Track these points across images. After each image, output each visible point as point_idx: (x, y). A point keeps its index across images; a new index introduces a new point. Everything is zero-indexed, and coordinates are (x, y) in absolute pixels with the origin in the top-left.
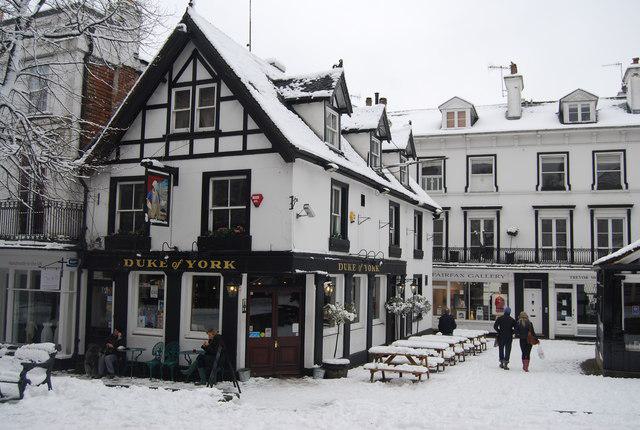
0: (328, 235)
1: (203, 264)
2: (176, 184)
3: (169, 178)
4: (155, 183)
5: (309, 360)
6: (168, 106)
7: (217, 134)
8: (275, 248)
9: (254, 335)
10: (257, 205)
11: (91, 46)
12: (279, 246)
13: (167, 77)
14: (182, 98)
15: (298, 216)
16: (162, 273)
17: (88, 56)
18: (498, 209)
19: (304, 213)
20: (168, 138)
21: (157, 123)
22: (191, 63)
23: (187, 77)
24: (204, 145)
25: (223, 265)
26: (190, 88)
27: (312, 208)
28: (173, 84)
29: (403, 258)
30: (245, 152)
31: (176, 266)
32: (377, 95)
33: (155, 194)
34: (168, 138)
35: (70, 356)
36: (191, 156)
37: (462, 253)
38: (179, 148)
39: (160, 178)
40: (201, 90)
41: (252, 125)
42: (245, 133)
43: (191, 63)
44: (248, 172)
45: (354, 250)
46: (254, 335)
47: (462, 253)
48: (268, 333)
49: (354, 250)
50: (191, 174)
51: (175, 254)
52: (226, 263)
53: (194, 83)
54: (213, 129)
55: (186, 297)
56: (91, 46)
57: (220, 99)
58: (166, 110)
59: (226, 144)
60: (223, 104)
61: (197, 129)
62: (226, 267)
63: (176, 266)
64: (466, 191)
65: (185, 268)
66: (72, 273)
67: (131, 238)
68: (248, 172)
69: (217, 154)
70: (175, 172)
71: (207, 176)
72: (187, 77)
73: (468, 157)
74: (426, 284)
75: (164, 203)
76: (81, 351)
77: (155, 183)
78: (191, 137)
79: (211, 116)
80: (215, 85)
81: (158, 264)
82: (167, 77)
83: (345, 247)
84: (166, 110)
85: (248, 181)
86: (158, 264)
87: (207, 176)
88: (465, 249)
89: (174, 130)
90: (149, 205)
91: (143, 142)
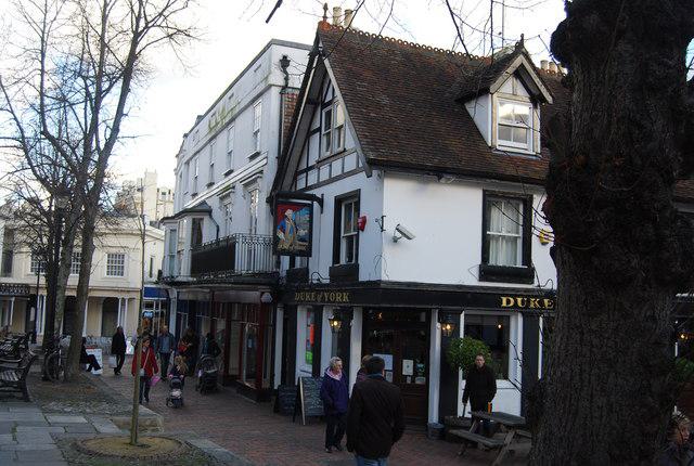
0: (479, 261)
3: (311, 206)
4: (289, 213)
5: (434, 416)
6: (319, 129)
11: (286, 79)
12: (373, 278)
15: (395, 240)
19: (398, 235)
20: (320, 162)
21: (314, 153)
27: (408, 227)
28: (325, 105)
33: (289, 225)
34: (320, 162)
36: (332, 180)
38: (324, 174)
51: (320, 288)
56: (286, 79)
69: (344, 175)
70: (321, 202)
72: (329, 98)
77: (289, 213)
85: (358, 204)
90: (281, 235)
91: (309, 169)
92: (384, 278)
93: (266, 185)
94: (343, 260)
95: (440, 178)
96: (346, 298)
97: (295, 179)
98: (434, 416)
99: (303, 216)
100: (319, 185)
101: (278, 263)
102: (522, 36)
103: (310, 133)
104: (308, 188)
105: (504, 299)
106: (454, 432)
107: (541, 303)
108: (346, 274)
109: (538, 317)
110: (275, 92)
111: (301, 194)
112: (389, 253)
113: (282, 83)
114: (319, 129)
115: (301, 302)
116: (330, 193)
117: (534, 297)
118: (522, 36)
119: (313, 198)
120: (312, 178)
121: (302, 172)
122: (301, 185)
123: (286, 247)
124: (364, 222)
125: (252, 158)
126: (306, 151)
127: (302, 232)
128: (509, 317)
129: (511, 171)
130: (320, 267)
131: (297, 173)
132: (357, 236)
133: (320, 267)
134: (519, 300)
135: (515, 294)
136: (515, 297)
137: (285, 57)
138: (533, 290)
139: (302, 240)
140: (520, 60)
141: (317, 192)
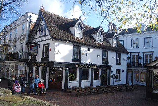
2: (40, 47)
3: (37, 46)
4: (33, 47)
5: (63, 88)
7: (45, 36)
18: (153, 52)
20: (39, 37)
21: (38, 34)
23: (42, 24)
24: (44, 38)
25: (45, 65)
28: (41, 26)
29: (109, 65)
30: (49, 39)
33: (33, 49)
34: (39, 37)
37: (143, 64)
38: (40, 39)
44: (49, 44)
46: (51, 81)
47: (143, 64)
50: (42, 44)
53: (43, 25)
55: (40, 72)
59: (47, 38)
64: (144, 47)
66: (26, 67)
67: (34, 59)
68: (49, 44)
69: (45, 40)
70: (39, 45)
71: (44, 45)
72: (42, 24)
73: (144, 38)
77: (33, 47)
78: (42, 37)
85: (49, 46)
87: (44, 45)
88: (144, 63)
90: (31, 52)
91: (36, 38)
92: (55, 61)
93: (25, 41)
94: (44, 56)
95: (66, 42)
96: (45, 65)
97: (33, 40)
98: (63, 88)
99: (36, 48)
100: (39, 42)
101: (28, 57)
102: (80, 16)
103: (37, 31)
104: (36, 42)
105: (76, 65)
106: (69, 91)
107: (82, 66)
108: (46, 59)
109: (82, 69)
111: (34, 43)
114: (39, 31)
116: (42, 44)
117: (81, 65)
118: (80, 16)
119: (38, 44)
120: (37, 40)
121: (35, 39)
122: (34, 41)
123: (32, 54)
125: (22, 35)
127: (36, 51)
129: (78, 41)
130: (39, 58)
131: (33, 39)
132: (48, 53)
133: (39, 58)
134: (79, 65)
135: (78, 64)
136: (78, 65)
137: (31, 15)
138: (81, 64)
140: (80, 21)
141: (39, 43)
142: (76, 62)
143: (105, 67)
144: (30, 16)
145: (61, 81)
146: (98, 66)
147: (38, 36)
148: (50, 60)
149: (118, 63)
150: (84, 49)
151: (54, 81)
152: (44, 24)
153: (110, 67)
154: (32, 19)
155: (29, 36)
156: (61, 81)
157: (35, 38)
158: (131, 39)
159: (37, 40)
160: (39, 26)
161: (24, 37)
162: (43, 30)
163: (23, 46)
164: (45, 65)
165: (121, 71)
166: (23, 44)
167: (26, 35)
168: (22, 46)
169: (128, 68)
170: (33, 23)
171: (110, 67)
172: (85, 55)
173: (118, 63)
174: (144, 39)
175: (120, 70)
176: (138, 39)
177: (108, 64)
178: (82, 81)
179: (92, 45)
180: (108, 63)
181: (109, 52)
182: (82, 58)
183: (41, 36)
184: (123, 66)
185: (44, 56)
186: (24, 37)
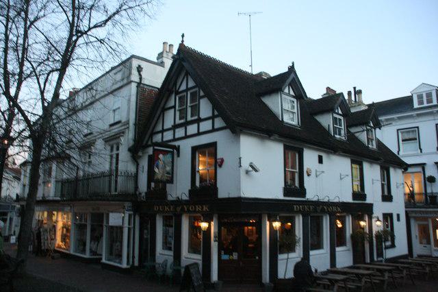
0: (283, 185)
1: (192, 208)
2: (178, 156)
3: (173, 153)
4: (161, 156)
6: (174, 107)
7: (199, 121)
8: (231, 196)
9: (225, 257)
10: (220, 166)
11: (141, 79)
12: (233, 195)
13: (174, 89)
14: (182, 101)
16: (171, 214)
17: (139, 84)
19: (250, 169)
20: (175, 127)
21: (170, 119)
22: (186, 78)
23: (183, 87)
24: (192, 129)
25: (202, 208)
26: (185, 94)
29: (368, 201)
30: (214, 130)
31: (179, 209)
32: (355, 88)
33: (160, 163)
34: (175, 127)
35: (129, 267)
36: (186, 137)
38: (180, 133)
39: (165, 153)
40: (191, 94)
41: (216, 113)
42: (213, 118)
43: (186, 78)
45: (311, 195)
46: (225, 257)
48: (235, 256)
49: (311, 195)
50: (186, 146)
51: (178, 202)
52: (204, 206)
53: (187, 89)
54: (196, 117)
56: (141, 79)
57: (201, 97)
58: (173, 110)
59: (206, 126)
60: (202, 101)
61: (189, 118)
62: (204, 209)
63: (179, 209)
65: (183, 211)
66: (130, 216)
69: (199, 134)
70: (178, 149)
71: (195, 150)
72: (183, 87)
74: (398, 220)
75: (168, 168)
76: (136, 263)
77: (161, 156)
78: (187, 123)
79: (195, 109)
80: (197, 89)
81: (170, 208)
82: (174, 89)
83: (302, 191)
84: (173, 110)
86: (170, 208)
89: (178, 121)
90: (156, 170)
91: (163, 131)
92: (242, 195)
93: (128, 139)
94: (198, 184)
96: (205, 208)
99: (168, 158)
100: (175, 140)
101: (136, 187)
102: (293, 63)
103: (165, 110)
105: (295, 207)
110: (134, 86)
111: (164, 144)
112: (244, 180)
113: (138, 80)
114: (174, 107)
115: (159, 212)
116: (186, 146)
118: (293, 63)
119: (174, 147)
124: (222, 160)
126: (161, 118)
128: (322, 217)
131: (154, 133)
137: (139, 66)
139: (168, 173)
141: (176, 143)
142: (295, 197)
143: (360, 207)
144: (139, 69)
145: (257, 258)
146: (344, 206)
147: (169, 122)
148: (223, 193)
149: (387, 198)
150: (310, 157)
151: (235, 256)
152: (192, 88)
153: (371, 205)
154: (143, 76)
155: (135, 124)
156: (257, 258)
157: (159, 128)
158: (398, 130)
159: (168, 136)
160: (173, 96)
161: (123, 128)
162: (189, 104)
163: (117, 155)
164: (205, 208)
165: (395, 218)
166: (118, 149)
167: (128, 124)
168: (115, 156)
169: (407, 209)
170: (145, 87)
171: (371, 205)
172: (313, 174)
173: (387, 198)
174: (398, 132)
175: (391, 215)
176: (418, 127)
177: (365, 200)
178: (312, 253)
179: (327, 145)
180: (364, 197)
181: (366, 166)
182: (308, 183)
183: (182, 121)
184: (397, 207)
185: (198, 184)
186: (123, 128)
